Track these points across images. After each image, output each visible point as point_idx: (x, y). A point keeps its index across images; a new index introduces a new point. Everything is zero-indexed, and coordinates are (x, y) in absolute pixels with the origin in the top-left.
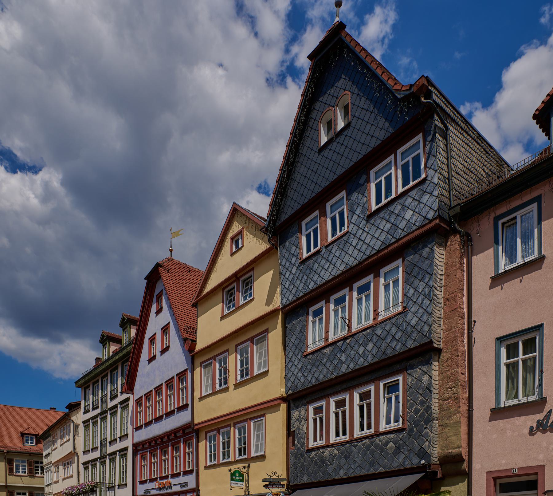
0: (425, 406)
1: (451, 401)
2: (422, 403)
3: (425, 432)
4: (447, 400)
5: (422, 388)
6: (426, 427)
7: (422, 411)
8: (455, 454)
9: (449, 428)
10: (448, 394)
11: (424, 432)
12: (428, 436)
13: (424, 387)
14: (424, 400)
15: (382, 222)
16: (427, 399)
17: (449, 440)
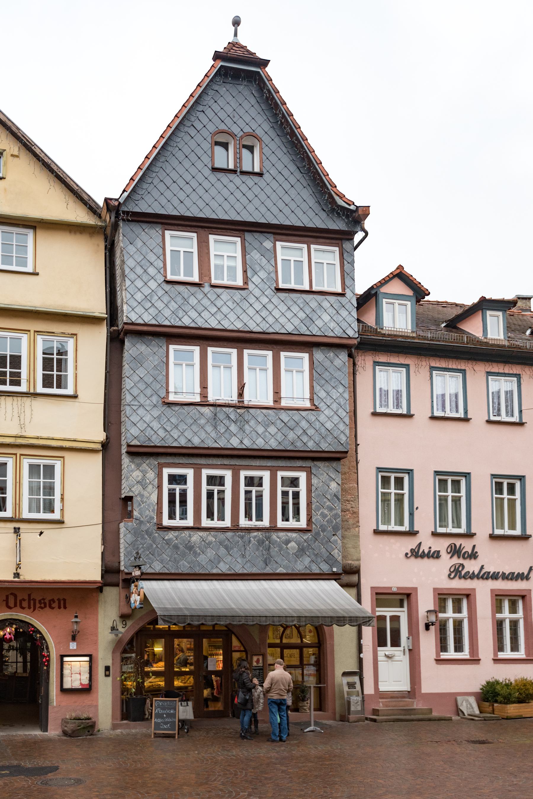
0: (333, 512)
1: (349, 513)
2: (331, 509)
3: (334, 539)
4: (345, 512)
5: (329, 494)
6: (334, 533)
7: (329, 517)
8: (354, 566)
9: (348, 540)
10: (346, 506)
11: (333, 539)
12: (337, 544)
13: (332, 493)
14: (332, 506)
16: (336, 505)
17: (347, 551)
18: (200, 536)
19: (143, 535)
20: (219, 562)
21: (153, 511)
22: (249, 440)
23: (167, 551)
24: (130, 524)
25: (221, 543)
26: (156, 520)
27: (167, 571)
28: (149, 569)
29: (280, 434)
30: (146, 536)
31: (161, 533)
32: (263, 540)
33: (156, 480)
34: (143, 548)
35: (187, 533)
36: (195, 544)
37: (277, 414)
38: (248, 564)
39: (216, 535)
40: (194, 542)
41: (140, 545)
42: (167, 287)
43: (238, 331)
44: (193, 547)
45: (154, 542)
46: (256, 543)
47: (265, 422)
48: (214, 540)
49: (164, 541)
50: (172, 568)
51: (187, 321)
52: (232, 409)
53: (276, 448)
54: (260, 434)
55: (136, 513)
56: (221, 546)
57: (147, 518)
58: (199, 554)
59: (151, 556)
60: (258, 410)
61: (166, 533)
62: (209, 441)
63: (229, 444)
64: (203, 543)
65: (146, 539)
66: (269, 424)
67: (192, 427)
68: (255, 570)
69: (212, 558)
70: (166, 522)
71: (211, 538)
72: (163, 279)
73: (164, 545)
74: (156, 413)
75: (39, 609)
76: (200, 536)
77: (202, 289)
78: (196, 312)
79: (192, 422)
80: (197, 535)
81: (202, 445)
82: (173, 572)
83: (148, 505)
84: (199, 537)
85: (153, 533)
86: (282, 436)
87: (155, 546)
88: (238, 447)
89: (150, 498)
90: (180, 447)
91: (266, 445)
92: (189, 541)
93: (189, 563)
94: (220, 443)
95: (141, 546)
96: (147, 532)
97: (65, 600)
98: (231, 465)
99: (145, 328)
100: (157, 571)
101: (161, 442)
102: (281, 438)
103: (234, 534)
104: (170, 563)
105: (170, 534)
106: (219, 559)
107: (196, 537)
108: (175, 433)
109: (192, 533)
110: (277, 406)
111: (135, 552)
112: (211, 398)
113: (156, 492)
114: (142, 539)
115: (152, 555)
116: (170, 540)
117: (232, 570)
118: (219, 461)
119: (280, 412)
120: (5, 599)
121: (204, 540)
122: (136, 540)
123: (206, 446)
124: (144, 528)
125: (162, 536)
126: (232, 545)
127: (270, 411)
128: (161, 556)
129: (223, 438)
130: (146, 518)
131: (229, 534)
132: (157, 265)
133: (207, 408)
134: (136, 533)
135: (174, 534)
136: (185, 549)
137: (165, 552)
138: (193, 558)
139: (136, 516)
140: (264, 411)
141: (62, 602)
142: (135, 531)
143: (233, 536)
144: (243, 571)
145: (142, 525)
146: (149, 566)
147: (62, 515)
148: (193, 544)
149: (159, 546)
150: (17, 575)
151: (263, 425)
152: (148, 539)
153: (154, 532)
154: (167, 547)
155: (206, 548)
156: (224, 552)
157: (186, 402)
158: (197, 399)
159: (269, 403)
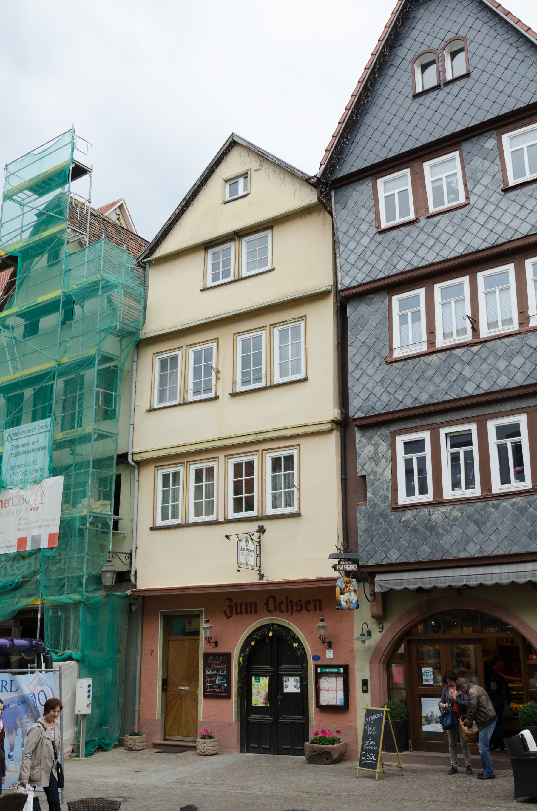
15: (529, 200)
18: (442, 512)
19: (378, 519)
20: (467, 544)
21: (387, 489)
22: (487, 381)
23: (405, 535)
24: (363, 508)
25: (469, 517)
26: (391, 499)
27: (405, 561)
28: (385, 559)
29: (528, 364)
30: (381, 520)
31: (397, 514)
32: (526, 507)
33: (389, 452)
34: (378, 534)
35: (426, 510)
36: (436, 523)
37: (522, 339)
38: (506, 542)
39: (462, 509)
40: (435, 521)
41: (375, 531)
42: (379, 238)
43: (462, 256)
44: (435, 527)
45: (390, 525)
46: (516, 512)
47: (507, 354)
48: (460, 514)
49: (401, 524)
50: (411, 555)
51: (402, 267)
52: (465, 349)
53: (524, 383)
54: (502, 370)
55: (369, 494)
56: (470, 522)
57: (381, 499)
58: (443, 535)
59: (387, 543)
60: (498, 340)
61: (402, 513)
62: (439, 394)
63: (464, 393)
64: (447, 520)
65: (381, 523)
66: (513, 354)
67: (418, 383)
68: (516, 550)
69: (459, 538)
70: (403, 499)
71: (456, 513)
72: (375, 230)
73: (401, 528)
74: (378, 377)
75: (297, 612)
76: (442, 512)
77: (417, 225)
78: (412, 252)
79: (418, 377)
80: (439, 511)
81: (431, 401)
82: (412, 560)
83: (382, 483)
84: (441, 513)
85: (388, 515)
86: (531, 366)
87: (391, 531)
88: (474, 394)
89: (384, 474)
90: (406, 409)
91: (510, 383)
92: (430, 520)
93: (430, 548)
94: (452, 394)
95: (376, 532)
96: (381, 514)
97: (320, 601)
98: (474, 417)
99: (361, 289)
100: (394, 561)
101: (385, 408)
102: (529, 369)
103: (485, 504)
104: (409, 549)
105: (407, 514)
106: (468, 540)
107: (437, 514)
108: (400, 394)
109: (432, 510)
110: (525, 328)
111: (370, 541)
112: (440, 343)
113: (390, 466)
114: (376, 524)
115: (389, 542)
116: (407, 521)
117: (484, 552)
118: (458, 416)
119: (526, 337)
120: (266, 603)
121: (447, 516)
122: (370, 527)
123: (436, 401)
124: (377, 511)
125: (398, 518)
126: (483, 518)
127: (513, 339)
128: (398, 543)
129: (456, 387)
130: (380, 498)
131: (480, 505)
132: (369, 218)
133: (434, 355)
134: (371, 517)
135: (411, 514)
136: (425, 531)
137: (402, 537)
138: (436, 541)
139: (369, 498)
140: (505, 340)
141: (317, 603)
142: (369, 516)
143: (485, 506)
144: (498, 551)
145: (376, 507)
146: (384, 556)
147: (299, 508)
148: (434, 523)
149: (395, 530)
150: (261, 576)
151: (506, 358)
152: (384, 523)
153: (390, 513)
154: (404, 530)
155: (451, 526)
156: (474, 529)
157: (409, 355)
158: (424, 348)
159: (514, 328)
